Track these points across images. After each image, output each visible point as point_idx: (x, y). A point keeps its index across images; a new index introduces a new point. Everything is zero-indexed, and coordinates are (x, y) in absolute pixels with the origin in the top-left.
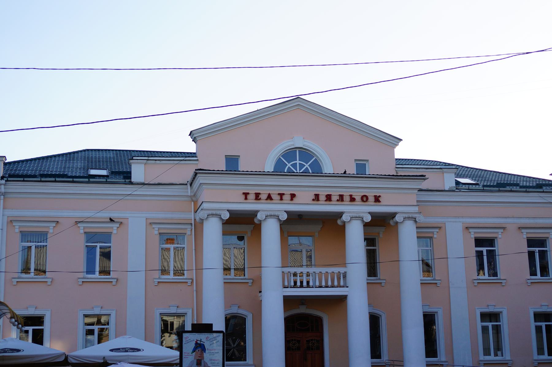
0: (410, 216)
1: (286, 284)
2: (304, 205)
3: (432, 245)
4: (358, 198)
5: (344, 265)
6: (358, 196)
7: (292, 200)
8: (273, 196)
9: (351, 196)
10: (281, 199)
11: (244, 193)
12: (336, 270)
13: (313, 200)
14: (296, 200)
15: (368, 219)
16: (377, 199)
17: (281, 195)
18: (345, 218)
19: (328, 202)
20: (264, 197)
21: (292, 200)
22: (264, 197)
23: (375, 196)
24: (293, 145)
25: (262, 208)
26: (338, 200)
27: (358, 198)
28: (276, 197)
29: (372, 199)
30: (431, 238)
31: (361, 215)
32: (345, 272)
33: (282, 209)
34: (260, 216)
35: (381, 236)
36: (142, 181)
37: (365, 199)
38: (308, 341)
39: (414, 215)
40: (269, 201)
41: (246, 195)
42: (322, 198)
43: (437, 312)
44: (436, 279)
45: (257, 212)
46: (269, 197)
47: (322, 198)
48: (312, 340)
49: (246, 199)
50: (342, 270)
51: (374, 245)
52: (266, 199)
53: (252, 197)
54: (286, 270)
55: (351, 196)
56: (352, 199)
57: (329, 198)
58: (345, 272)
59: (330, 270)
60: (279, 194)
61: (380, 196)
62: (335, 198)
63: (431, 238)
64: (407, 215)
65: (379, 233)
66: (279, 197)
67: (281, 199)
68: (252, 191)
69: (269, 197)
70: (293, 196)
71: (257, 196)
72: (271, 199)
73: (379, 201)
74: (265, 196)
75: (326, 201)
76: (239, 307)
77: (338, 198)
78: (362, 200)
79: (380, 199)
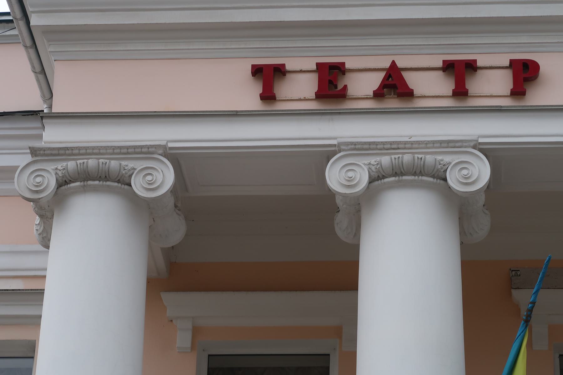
8: (414, 81)
10: (460, 92)
11: (257, 71)
17: (460, 72)
20: (363, 85)
21: (518, 92)
22: (363, 85)
28: (431, 86)
40: (392, 103)
41: (268, 77)
46: (394, 85)
49: (268, 96)
52: (378, 95)
53: (300, 88)
60: (449, 67)
67: (460, 92)
68: (302, 62)
69: (394, 85)
70: (525, 74)
71: (331, 83)
72: (406, 93)
74: (375, 81)
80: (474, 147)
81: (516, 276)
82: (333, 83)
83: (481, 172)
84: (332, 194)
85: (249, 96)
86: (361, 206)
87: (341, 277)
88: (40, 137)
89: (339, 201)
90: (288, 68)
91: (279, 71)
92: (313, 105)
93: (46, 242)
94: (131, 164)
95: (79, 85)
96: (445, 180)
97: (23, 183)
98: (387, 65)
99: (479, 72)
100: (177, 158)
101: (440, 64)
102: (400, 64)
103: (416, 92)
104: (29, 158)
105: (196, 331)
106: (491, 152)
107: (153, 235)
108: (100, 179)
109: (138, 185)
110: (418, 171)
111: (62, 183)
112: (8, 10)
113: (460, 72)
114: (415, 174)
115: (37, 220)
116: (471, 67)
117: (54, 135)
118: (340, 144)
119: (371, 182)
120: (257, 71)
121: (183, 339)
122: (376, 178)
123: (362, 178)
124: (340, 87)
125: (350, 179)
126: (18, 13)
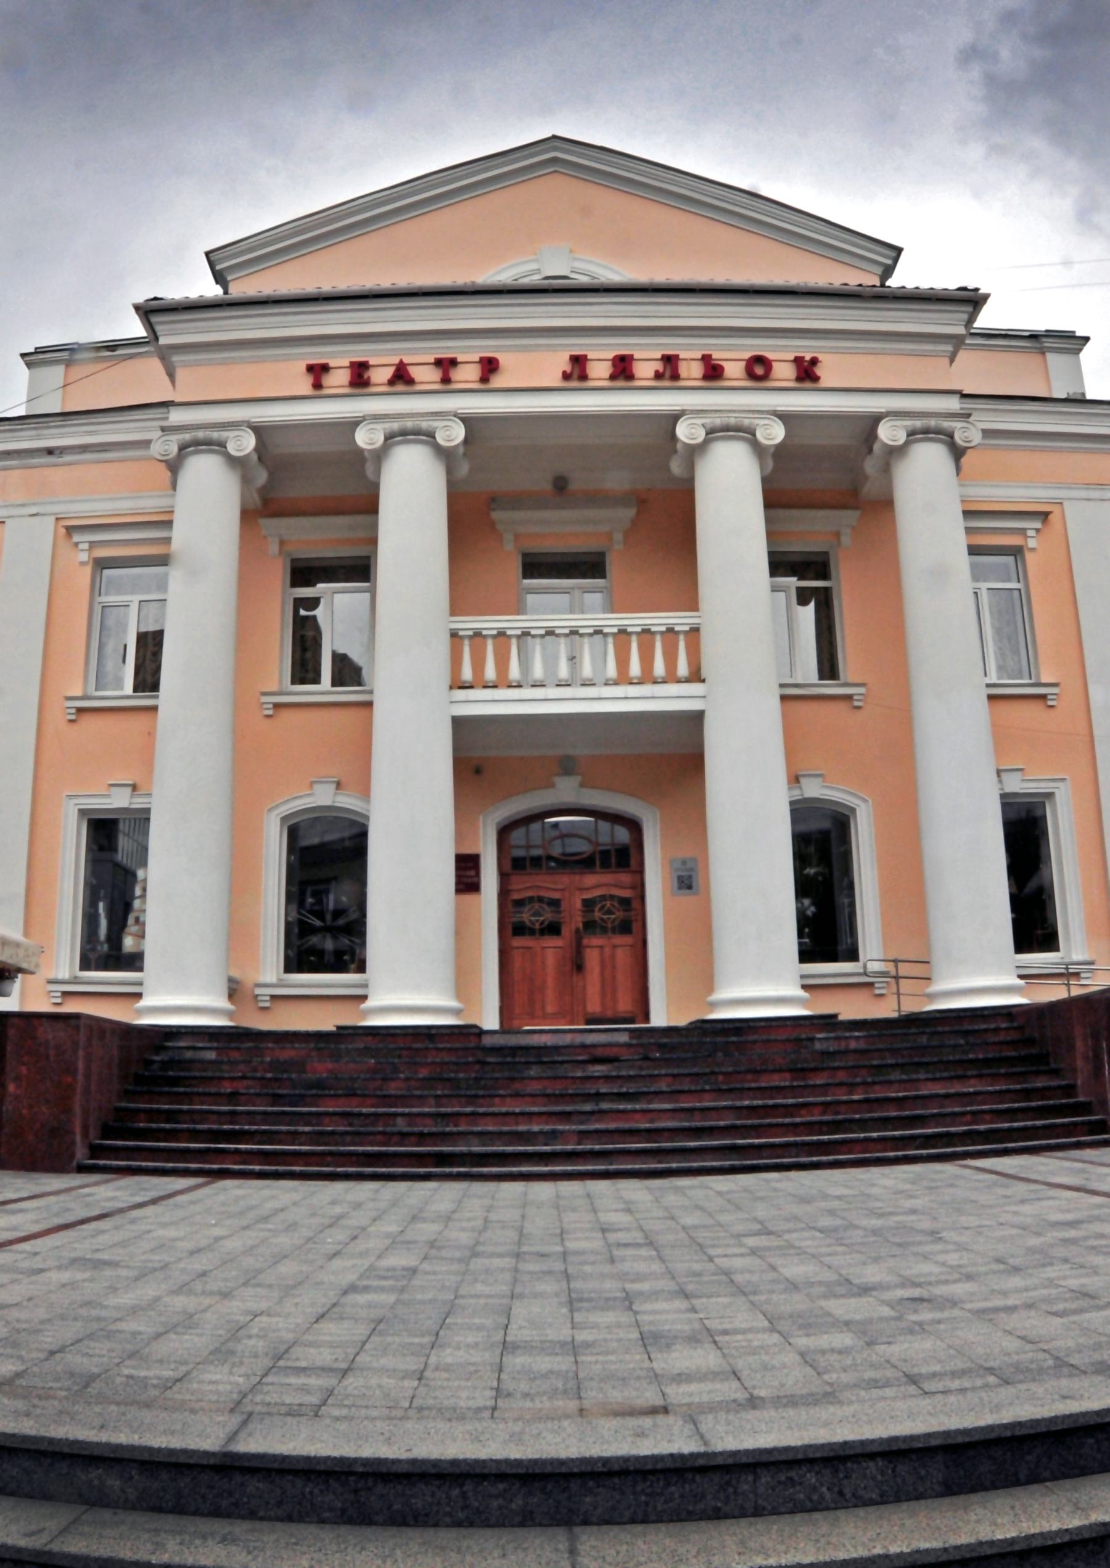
0: (932, 423)
1: (467, 674)
2: (532, 389)
3: (1022, 574)
4: (734, 370)
5: (693, 604)
6: (734, 359)
7: (484, 379)
8: (415, 372)
9: (706, 359)
10: (446, 380)
11: (310, 368)
12: (658, 620)
13: (566, 376)
14: (497, 381)
15: (774, 433)
16: (807, 373)
17: (446, 365)
18: (685, 432)
19: (621, 383)
20: (380, 376)
21: (484, 379)
23: (798, 361)
24: (538, 271)
25: (371, 414)
26: (658, 376)
27: (734, 370)
29: (784, 372)
30: (1016, 552)
31: (746, 422)
32: (695, 631)
33: (448, 411)
34: (366, 438)
35: (846, 540)
36: (58, 411)
37: (758, 370)
38: (588, 904)
39: (946, 424)
40: (400, 387)
41: (318, 371)
42: (600, 370)
43: (1050, 795)
44: (1044, 680)
45: (353, 424)
46: (401, 376)
47: (600, 370)
48: (603, 898)
49: (317, 385)
50: (680, 620)
51: (824, 574)
52: (391, 382)
53: (339, 379)
54: (467, 624)
55: (706, 359)
56: (713, 372)
57: (623, 368)
58: (694, 631)
59: (635, 621)
60: (439, 363)
61: (814, 361)
62: (644, 370)
63: (1016, 552)
64: (918, 424)
65: (837, 535)
66: (435, 375)
67: (446, 380)
68: (340, 359)
69: (401, 376)
70: (490, 367)
71: (360, 376)
72: (410, 381)
73: (815, 379)
74: (389, 372)
75: (613, 377)
76: (339, 785)
77: (659, 366)
78: (751, 375)
79: (819, 371)
80: (455, 416)
81: (494, 501)
82: (360, 376)
83: (458, 433)
84: (360, 452)
85: (304, 386)
86: (380, 455)
87: (367, 505)
88: (167, 418)
89: (366, 454)
90: (332, 365)
91: (325, 368)
92: (347, 390)
93: (174, 486)
94: (224, 434)
95: (194, 381)
96: (434, 438)
97: (156, 449)
98: (397, 361)
99: (460, 366)
100: (258, 430)
101: (432, 361)
102: (406, 361)
103: (417, 380)
104: (160, 433)
105: (282, 543)
106: (467, 420)
107: (246, 480)
108: (206, 444)
109: (231, 449)
110: (417, 432)
111: (182, 448)
112: (145, 334)
113: (446, 365)
114: (414, 434)
115: (169, 474)
116: (453, 362)
117: (176, 417)
118: (363, 417)
119: (387, 439)
120: (310, 368)
121: (274, 548)
122: (389, 437)
123: (380, 440)
124: (366, 377)
125: (371, 439)
126: (152, 336)
